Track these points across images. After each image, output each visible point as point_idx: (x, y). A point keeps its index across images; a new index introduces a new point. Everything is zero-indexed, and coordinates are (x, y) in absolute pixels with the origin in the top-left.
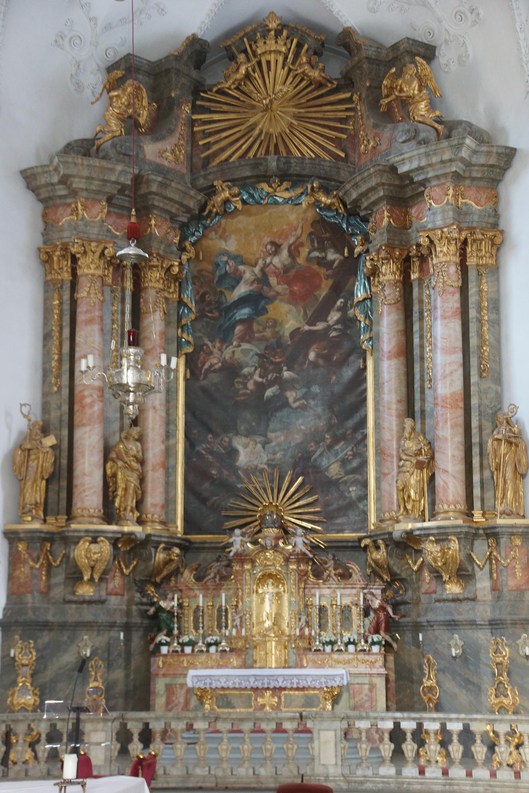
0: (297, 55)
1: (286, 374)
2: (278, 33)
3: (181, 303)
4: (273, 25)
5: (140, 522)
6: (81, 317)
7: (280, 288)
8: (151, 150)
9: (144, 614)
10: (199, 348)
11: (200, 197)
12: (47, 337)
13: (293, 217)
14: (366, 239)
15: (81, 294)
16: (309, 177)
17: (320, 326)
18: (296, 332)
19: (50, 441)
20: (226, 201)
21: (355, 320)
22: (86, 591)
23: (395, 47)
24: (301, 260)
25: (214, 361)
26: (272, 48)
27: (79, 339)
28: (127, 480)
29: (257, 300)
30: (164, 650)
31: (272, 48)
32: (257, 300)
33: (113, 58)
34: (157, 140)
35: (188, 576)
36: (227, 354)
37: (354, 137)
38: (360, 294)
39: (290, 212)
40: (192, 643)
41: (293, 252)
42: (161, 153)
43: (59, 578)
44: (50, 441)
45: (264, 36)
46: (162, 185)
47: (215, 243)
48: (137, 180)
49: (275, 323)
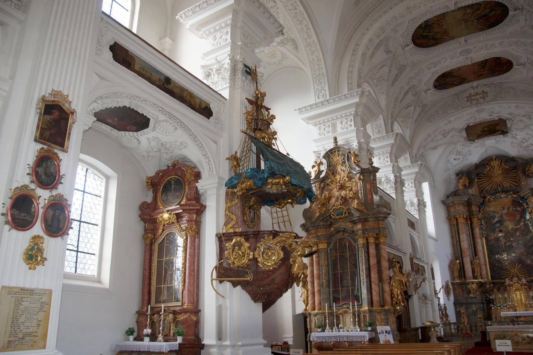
0: (501, 163)
1: (512, 239)
2: (496, 160)
3: (481, 224)
4: (494, 158)
5: (482, 278)
6: (460, 232)
7: (506, 218)
8: (470, 191)
9: (486, 300)
10: (488, 235)
11: (483, 199)
12: (452, 237)
13: (506, 201)
14: (527, 204)
15: (460, 226)
16: (509, 191)
17: (519, 226)
18: (512, 229)
19: (458, 261)
20: (489, 199)
21: (528, 224)
22: (471, 295)
23: (527, 160)
24: (510, 211)
25: (492, 237)
26: (495, 163)
27: (461, 237)
28: (477, 269)
29: (500, 222)
30: (493, 308)
31: (495, 163)
32: (500, 222)
33: (457, 172)
34: (471, 188)
35: (495, 290)
36: (495, 236)
37: (519, 180)
38: (528, 217)
39: (506, 199)
40: (499, 306)
41: (508, 209)
42: (472, 191)
43: (465, 293)
44: (458, 261)
45: (492, 160)
46: (475, 199)
47: (487, 209)
48: (468, 199)
49: (507, 227)
